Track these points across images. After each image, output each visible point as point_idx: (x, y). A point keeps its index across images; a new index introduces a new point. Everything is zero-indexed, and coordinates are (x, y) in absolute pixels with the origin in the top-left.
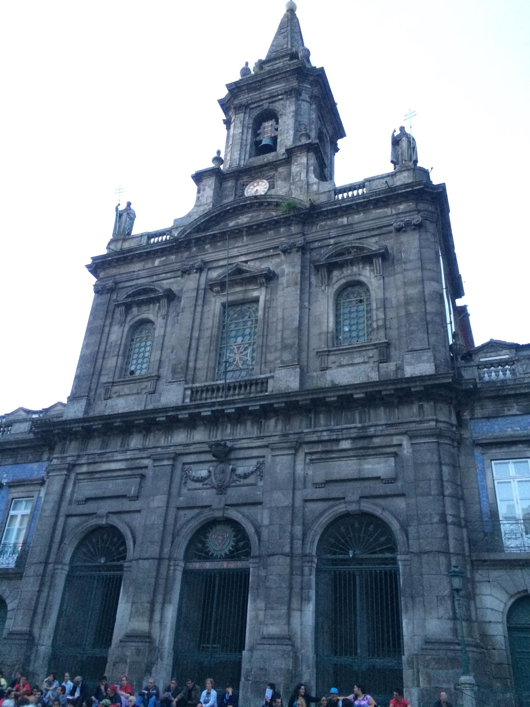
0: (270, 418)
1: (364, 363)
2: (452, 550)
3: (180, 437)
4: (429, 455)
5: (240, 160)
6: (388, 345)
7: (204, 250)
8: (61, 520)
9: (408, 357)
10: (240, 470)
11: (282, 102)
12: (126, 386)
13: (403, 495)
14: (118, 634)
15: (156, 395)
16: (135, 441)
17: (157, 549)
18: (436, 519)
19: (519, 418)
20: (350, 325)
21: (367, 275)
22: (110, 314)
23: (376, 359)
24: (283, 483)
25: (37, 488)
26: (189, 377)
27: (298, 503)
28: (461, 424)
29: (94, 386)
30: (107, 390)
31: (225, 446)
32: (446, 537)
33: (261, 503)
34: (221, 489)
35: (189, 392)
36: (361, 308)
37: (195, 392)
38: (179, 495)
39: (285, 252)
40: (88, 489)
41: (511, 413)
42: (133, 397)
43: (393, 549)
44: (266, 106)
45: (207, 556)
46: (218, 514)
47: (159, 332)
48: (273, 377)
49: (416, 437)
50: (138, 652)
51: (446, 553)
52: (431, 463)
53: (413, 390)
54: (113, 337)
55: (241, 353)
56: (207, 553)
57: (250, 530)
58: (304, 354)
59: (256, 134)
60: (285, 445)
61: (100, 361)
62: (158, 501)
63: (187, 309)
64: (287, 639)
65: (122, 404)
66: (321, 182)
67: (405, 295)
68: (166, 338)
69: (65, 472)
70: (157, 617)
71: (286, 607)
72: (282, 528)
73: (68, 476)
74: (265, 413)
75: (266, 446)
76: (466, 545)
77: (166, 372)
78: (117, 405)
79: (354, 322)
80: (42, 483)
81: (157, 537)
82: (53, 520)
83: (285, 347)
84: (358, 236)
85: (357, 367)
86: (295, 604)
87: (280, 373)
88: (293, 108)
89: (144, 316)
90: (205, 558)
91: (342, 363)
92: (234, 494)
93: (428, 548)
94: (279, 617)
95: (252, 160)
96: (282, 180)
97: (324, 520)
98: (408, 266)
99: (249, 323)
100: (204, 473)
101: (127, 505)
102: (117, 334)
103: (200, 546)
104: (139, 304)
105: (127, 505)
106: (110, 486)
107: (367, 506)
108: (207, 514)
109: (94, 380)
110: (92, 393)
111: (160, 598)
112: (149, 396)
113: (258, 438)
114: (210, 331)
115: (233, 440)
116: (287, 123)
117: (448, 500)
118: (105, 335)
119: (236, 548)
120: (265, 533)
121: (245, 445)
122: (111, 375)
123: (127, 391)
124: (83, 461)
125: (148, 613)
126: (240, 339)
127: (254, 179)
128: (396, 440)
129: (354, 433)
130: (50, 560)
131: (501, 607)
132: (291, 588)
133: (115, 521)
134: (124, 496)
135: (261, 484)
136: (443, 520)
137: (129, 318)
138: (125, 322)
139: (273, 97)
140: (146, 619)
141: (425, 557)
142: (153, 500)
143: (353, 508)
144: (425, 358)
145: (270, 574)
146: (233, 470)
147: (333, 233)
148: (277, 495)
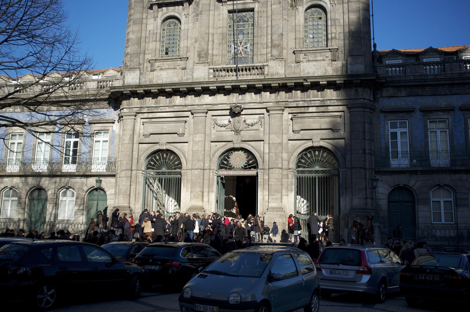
1: (323, 60)
2: (367, 167)
8: (136, 146)
10: (248, 122)
12: (165, 63)
17: (202, 164)
18: (361, 151)
19: (405, 98)
28: (375, 99)
30: (152, 65)
32: (365, 161)
34: (237, 132)
35: (212, 71)
36: (320, 23)
37: (215, 70)
41: (401, 95)
42: (172, 71)
45: (231, 168)
48: (268, 65)
49: (353, 107)
51: (365, 168)
53: (354, 81)
54: (150, 27)
55: (242, 46)
56: (229, 166)
58: (285, 51)
60: (277, 108)
61: (143, 44)
62: (199, 137)
63: (203, 13)
64: (281, 209)
65: (165, 76)
68: (189, 31)
69: (133, 117)
70: (206, 199)
71: (280, 194)
72: (276, 154)
76: (373, 164)
78: (161, 75)
79: (315, 31)
81: (201, 158)
82: (131, 145)
85: (319, 63)
86: (284, 192)
90: (229, 169)
91: (310, 59)
94: (277, 199)
100: (226, 122)
103: (225, 162)
106: (165, 127)
108: (230, 146)
111: (206, 190)
113: (260, 103)
114: (221, 29)
118: (144, 26)
122: (153, 55)
125: (201, 197)
129: (318, 103)
130: (133, 169)
131: (387, 192)
132: (282, 185)
134: (176, 133)
136: (364, 152)
140: (200, 199)
142: (196, 137)
143: (316, 144)
144: (359, 61)
146: (245, 121)
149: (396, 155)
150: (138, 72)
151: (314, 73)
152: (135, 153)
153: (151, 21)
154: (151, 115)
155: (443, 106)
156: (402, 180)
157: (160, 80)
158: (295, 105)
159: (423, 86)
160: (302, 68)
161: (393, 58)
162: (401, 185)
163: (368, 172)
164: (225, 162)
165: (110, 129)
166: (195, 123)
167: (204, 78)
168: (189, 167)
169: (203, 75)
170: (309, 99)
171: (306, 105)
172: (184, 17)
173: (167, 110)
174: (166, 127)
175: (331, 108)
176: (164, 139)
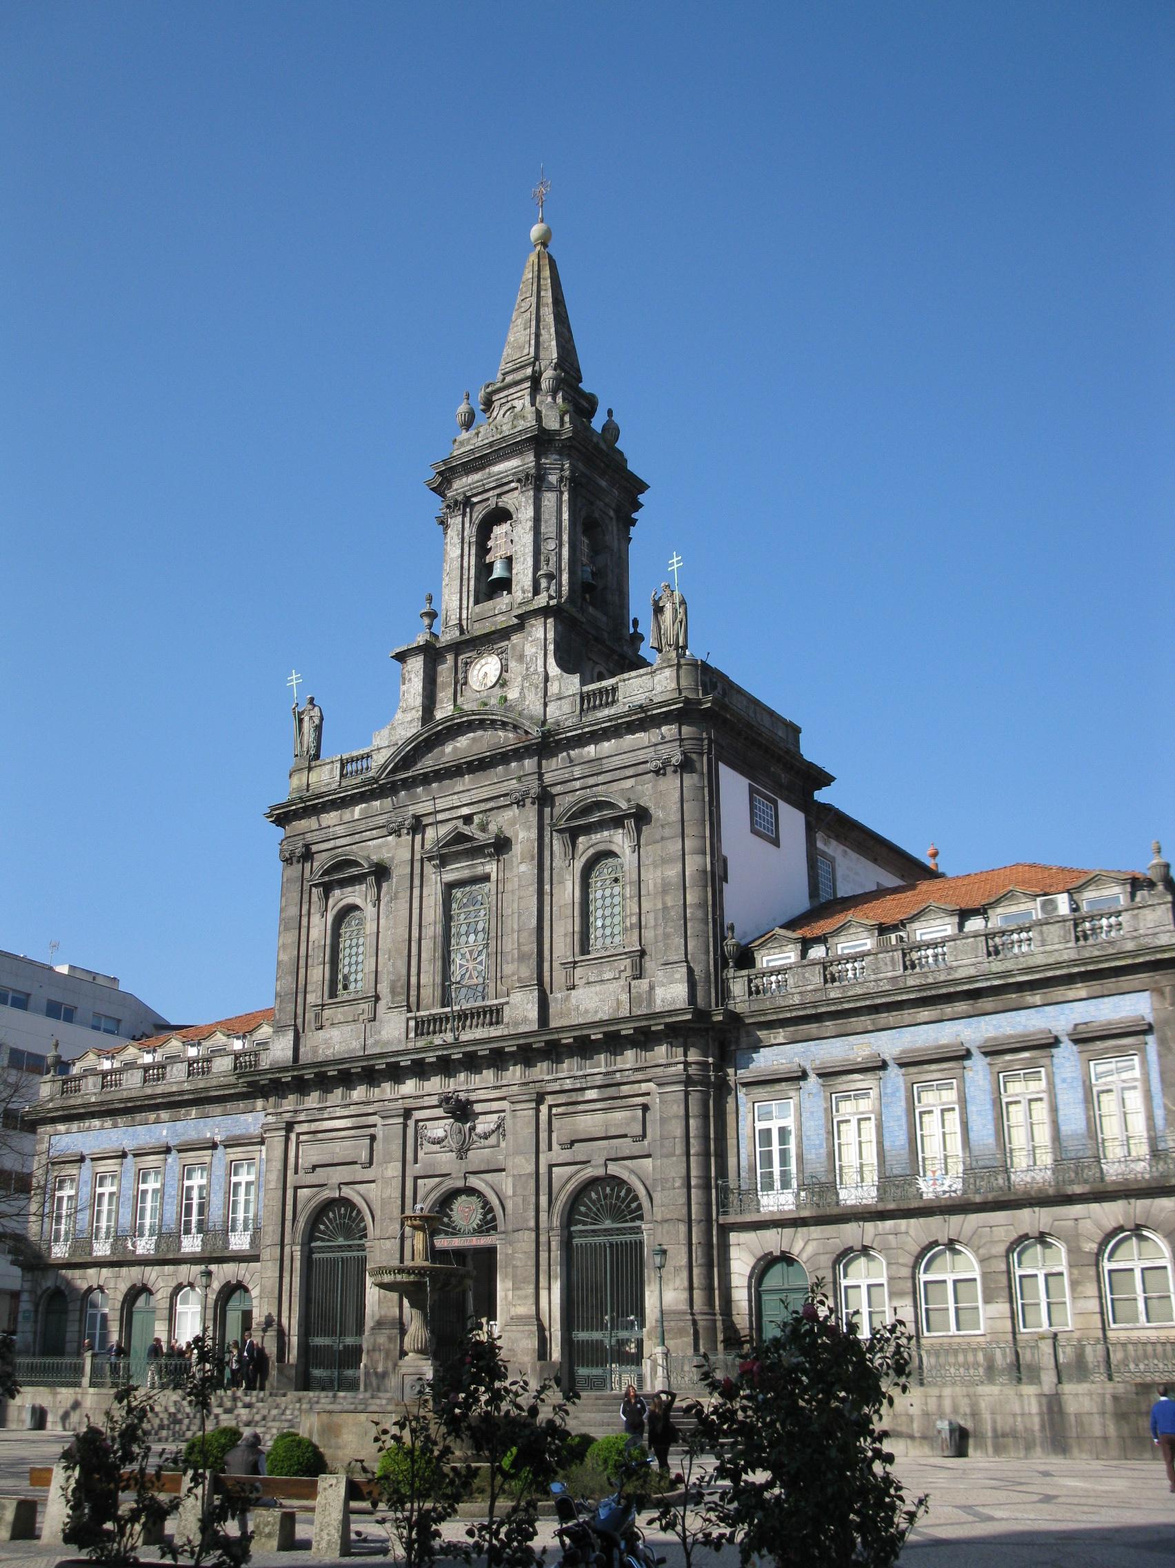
0: (508, 1061)
3: (409, 1086)
4: (675, 1107)
5: (461, 608)
6: (643, 953)
7: (416, 796)
8: (290, 1192)
9: (660, 973)
10: (480, 1129)
11: (516, 493)
13: (649, 1156)
14: (369, 1323)
15: (377, 1023)
16: (359, 1093)
20: (604, 917)
21: (620, 840)
22: (306, 896)
23: (628, 973)
24: (517, 1152)
25: (257, 1147)
26: (413, 999)
27: (543, 1169)
29: (300, 1011)
31: (458, 1101)
33: (503, 1170)
34: (462, 1152)
35: (412, 1023)
36: (617, 890)
38: (416, 1162)
39: (520, 803)
40: (310, 1154)
41: (778, 1041)
43: (641, 1218)
44: (492, 503)
45: (455, 1232)
46: (460, 1184)
47: (370, 927)
48: (507, 1003)
50: (390, 1339)
52: (677, 1117)
54: (315, 933)
56: (454, 1228)
57: (495, 1202)
59: (483, 549)
61: (302, 971)
62: (394, 1169)
63: (400, 895)
66: (565, 675)
67: (663, 879)
73: (287, 1139)
74: (498, 1059)
75: (503, 1099)
77: (384, 989)
78: (331, 1038)
80: (262, 1143)
82: (280, 1193)
83: (522, 958)
84: (607, 777)
87: (517, 997)
88: (530, 512)
89: (350, 900)
90: (453, 1234)
91: (592, 979)
92: (476, 1157)
93: (668, 1217)
94: (526, 1297)
95: (478, 608)
96: (516, 661)
97: (570, 1187)
98: (667, 832)
99: (482, 912)
100: (440, 1133)
101: (358, 1173)
102: (319, 928)
104: (343, 883)
105: (358, 1173)
106: (338, 1150)
107: (613, 1169)
108: (449, 1184)
109: (300, 1000)
110: (300, 1021)
112: (368, 1025)
115: (468, 1091)
116: (524, 540)
117: (692, 1158)
119: (485, 1221)
120: (509, 1205)
121: (483, 1097)
122: (320, 993)
123: (341, 1018)
124: (302, 1117)
126: (472, 937)
127: (480, 655)
128: (644, 1087)
129: (599, 1080)
133: (347, 1192)
134: (355, 1163)
135: (503, 1144)
137: (331, 902)
138: (326, 910)
139: (501, 486)
141: (666, 1225)
143: (600, 1172)
144: (677, 976)
145: (514, 1253)
146: (473, 1129)
147: (577, 772)
148: (520, 1160)
149: (769, 1186)
150: (290, 1035)
151: (596, 1012)
152: (289, 1208)
153: (316, 919)
154: (314, 1126)
155: (859, 1059)
156: (772, 1241)
157: (329, 1048)
158: (558, 1088)
159: (817, 1018)
160: (574, 1001)
161: (777, 950)
162: (777, 1253)
163: (694, 1230)
164: (446, 1220)
165: (257, 1155)
166: (386, 1139)
167: (400, 1041)
168: (378, 1233)
169: (396, 1033)
170: (581, 1073)
171: (578, 1086)
172: (370, 905)
173: (338, 1114)
174: (340, 1150)
175: (625, 1090)
176: (337, 1175)
